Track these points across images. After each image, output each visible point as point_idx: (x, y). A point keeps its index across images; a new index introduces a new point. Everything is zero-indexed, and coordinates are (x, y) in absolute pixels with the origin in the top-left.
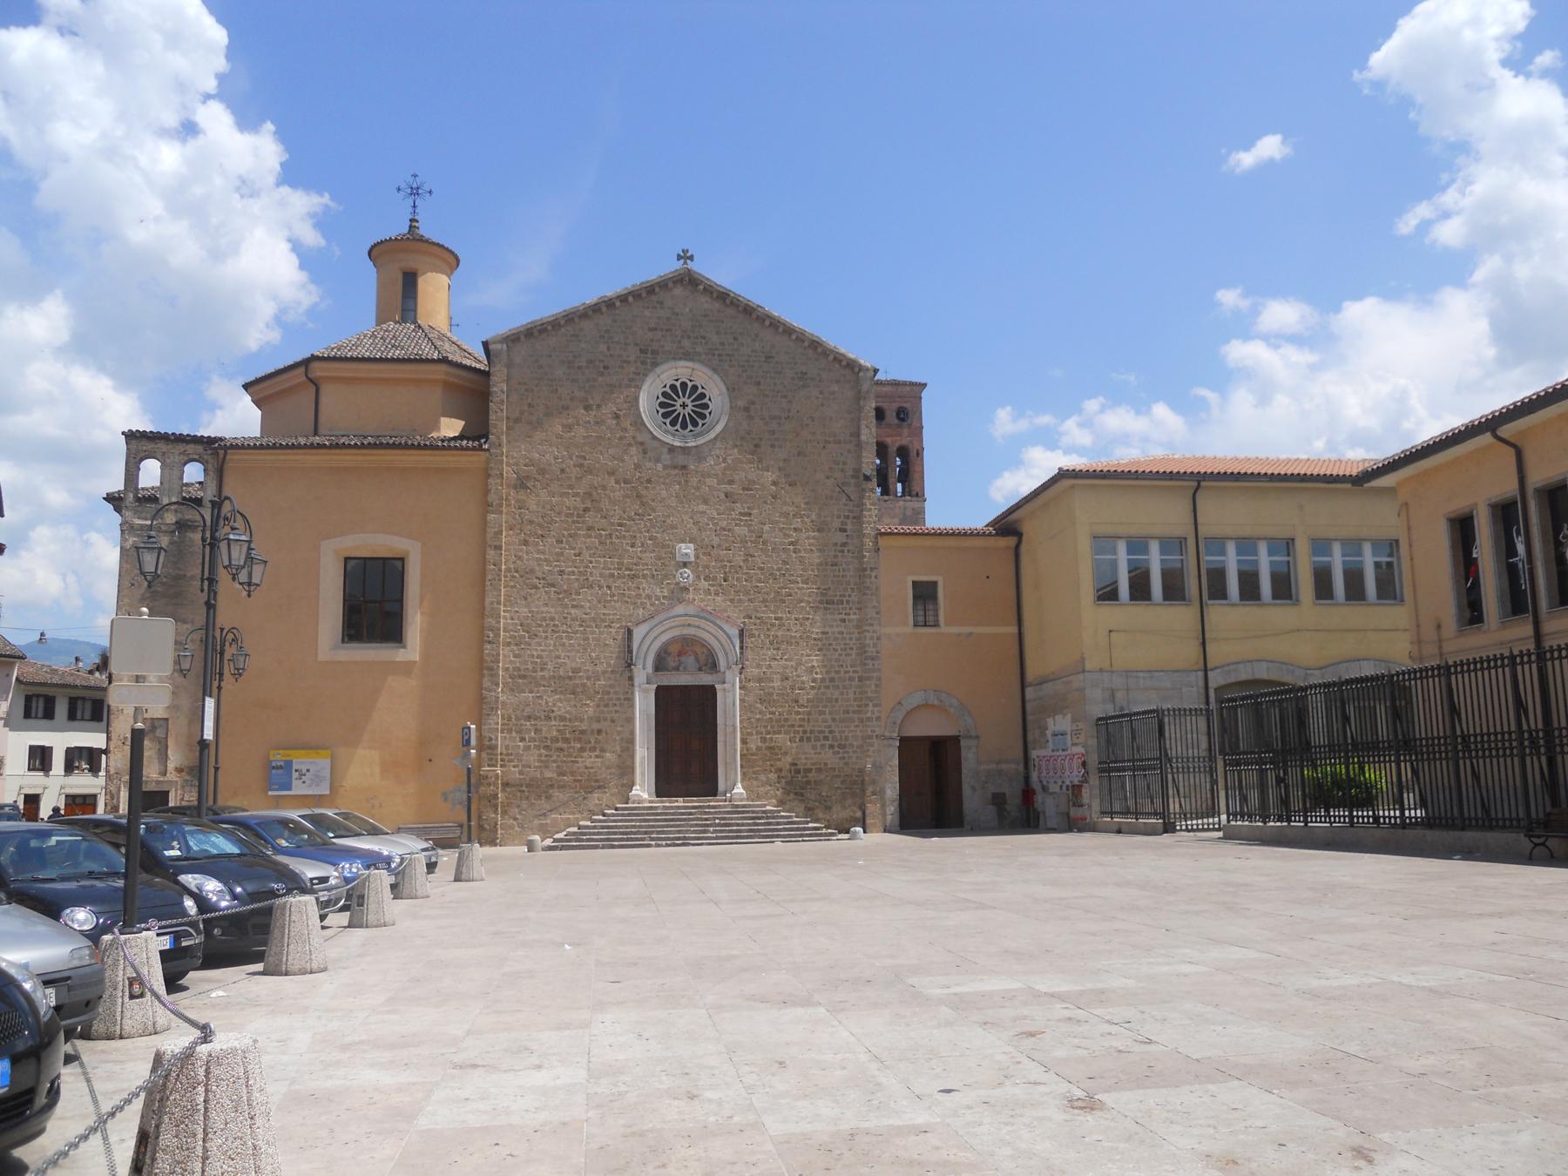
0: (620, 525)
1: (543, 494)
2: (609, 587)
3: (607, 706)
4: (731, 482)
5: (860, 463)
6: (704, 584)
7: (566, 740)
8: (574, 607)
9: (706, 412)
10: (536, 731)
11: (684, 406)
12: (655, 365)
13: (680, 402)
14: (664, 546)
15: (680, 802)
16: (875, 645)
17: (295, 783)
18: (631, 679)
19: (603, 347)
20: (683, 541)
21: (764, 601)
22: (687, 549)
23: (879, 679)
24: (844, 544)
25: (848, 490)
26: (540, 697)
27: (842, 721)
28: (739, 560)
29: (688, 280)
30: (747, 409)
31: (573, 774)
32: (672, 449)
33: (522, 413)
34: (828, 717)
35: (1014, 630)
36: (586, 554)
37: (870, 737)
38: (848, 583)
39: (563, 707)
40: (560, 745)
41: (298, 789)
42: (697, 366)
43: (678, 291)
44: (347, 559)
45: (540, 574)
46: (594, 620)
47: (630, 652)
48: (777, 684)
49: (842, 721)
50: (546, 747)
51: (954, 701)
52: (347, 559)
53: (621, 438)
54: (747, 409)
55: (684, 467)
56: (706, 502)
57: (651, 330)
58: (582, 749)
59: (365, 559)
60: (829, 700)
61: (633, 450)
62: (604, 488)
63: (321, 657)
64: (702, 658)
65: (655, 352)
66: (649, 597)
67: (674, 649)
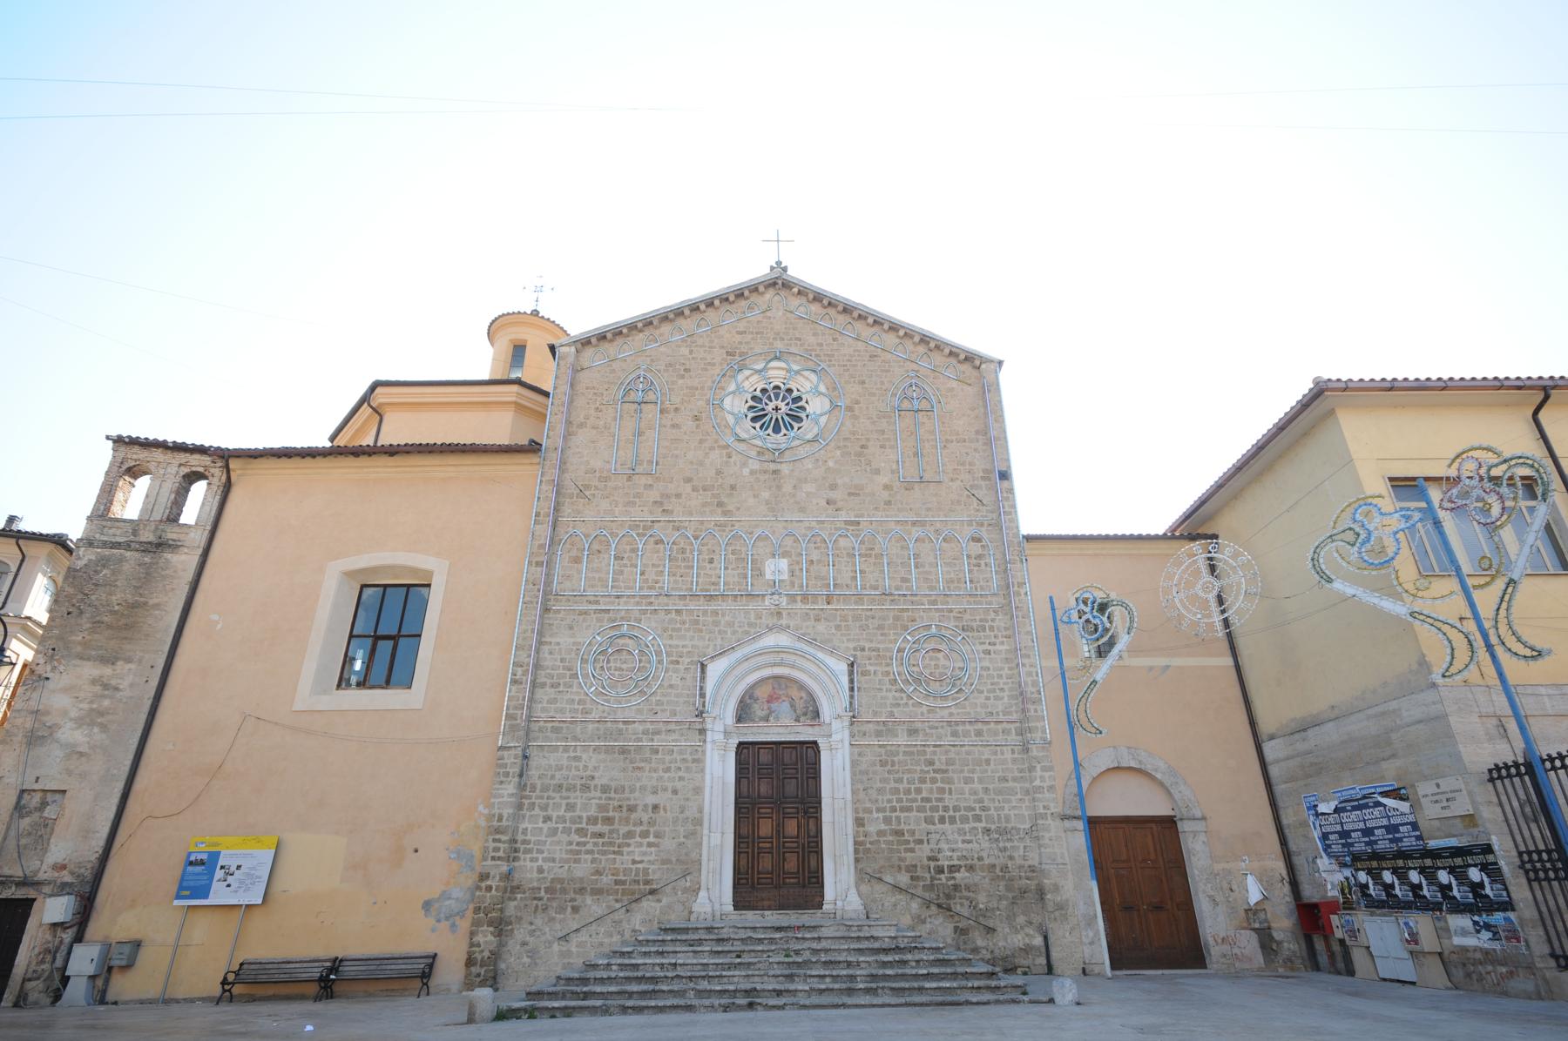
1: (605, 505)
3: (668, 770)
4: (833, 487)
7: (608, 820)
10: (570, 807)
17: (217, 887)
19: (685, 351)
21: (880, 627)
22: (776, 568)
24: (979, 557)
25: (980, 494)
27: (999, 792)
29: (779, 282)
30: (849, 409)
34: (977, 786)
35: (1230, 661)
37: (1044, 816)
39: (607, 772)
40: (599, 828)
41: (219, 894)
44: (363, 587)
47: (703, 695)
49: (999, 792)
50: (580, 832)
51: (1162, 765)
53: (701, 441)
54: (849, 409)
56: (802, 510)
57: (739, 333)
58: (630, 835)
59: (385, 586)
60: (978, 763)
64: (800, 705)
66: (730, 624)
67: (763, 693)
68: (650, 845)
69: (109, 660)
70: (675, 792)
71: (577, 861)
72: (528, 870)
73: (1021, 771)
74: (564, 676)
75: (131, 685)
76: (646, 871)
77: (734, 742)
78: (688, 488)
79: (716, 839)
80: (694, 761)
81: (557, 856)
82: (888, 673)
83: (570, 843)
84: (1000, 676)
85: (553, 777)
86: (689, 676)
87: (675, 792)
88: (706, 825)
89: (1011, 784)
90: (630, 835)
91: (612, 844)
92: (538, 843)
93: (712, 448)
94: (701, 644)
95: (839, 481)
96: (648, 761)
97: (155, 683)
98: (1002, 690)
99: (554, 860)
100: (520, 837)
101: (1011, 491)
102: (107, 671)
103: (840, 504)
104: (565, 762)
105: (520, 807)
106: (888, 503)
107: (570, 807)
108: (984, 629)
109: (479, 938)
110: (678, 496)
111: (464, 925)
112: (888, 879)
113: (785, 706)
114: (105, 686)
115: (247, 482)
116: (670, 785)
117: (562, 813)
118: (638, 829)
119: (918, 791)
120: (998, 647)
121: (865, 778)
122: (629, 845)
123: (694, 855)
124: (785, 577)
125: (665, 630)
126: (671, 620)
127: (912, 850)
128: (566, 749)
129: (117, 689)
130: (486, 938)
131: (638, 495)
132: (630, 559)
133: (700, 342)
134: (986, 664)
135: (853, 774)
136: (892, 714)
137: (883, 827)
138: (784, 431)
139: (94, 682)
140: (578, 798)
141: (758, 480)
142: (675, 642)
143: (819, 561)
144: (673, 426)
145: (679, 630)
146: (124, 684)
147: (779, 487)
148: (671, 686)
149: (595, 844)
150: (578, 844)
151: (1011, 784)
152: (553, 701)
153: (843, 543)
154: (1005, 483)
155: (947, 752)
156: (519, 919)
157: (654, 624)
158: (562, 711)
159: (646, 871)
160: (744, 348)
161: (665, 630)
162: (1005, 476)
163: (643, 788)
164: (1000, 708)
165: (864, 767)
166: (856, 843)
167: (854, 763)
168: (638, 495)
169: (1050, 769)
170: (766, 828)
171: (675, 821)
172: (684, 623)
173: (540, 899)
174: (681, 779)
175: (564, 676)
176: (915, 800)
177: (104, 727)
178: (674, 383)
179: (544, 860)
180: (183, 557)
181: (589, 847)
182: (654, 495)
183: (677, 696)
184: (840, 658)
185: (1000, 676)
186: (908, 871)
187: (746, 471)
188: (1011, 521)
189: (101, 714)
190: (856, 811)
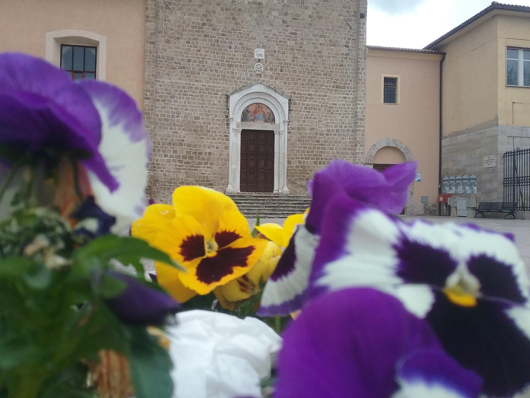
0: (223, 35)
1: (179, 13)
2: (216, 71)
3: (214, 139)
4: (286, 14)
5: (359, 8)
6: (269, 73)
7: (191, 158)
8: (196, 81)
10: (175, 152)
14: (247, 49)
15: (254, 194)
16: (362, 112)
18: (228, 124)
20: (258, 47)
21: (303, 84)
23: (364, 131)
24: (347, 54)
25: (351, 24)
26: (176, 133)
28: (289, 60)
36: (203, 52)
38: (348, 76)
40: (187, 160)
45: (177, 61)
46: (207, 89)
48: (308, 131)
50: (180, 161)
56: (272, 25)
58: (200, 163)
60: (336, 142)
62: (214, 12)
66: (239, 78)
67: (252, 109)
68: (208, 167)
70: (217, 148)
71: (180, 172)
72: (160, 174)
73: (352, 146)
74: (167, 97)
76: (207, 177)
78: (218, 9)
80: (225, 136)
82: (304, 104)
84: (349, 108)
85: (167, 139)
87: (217, 148)
89: (347, 151)
94: (226, 86)
95: (289, 12)
98: (349, 114)
99: (170, 172)
101: (364, 24)
103: (288, 23)
106: (310, 25)
107: (175, 152)
108: (345, 88)
112: (298, 183)
113: (261, 116)
116: (215, 145)
117: (172, 154)
118: (203, 162)
119: (312, 152)
120: (350, 96)
121: (292, 146)
122: (200, 167)
123: (226, 172)
124: (263, 58)
126: (213, 75)
127: (308, 174)
128: (171, 129)
131: (195, 10)
132: (193, 43)
134: (344, 103)
135: (288, 144)
136: (304, 122)
137: (298, 164)
140: (178, 148)
141: (251, 7)
143: (278, 51)
145: (217, 79)
147: (261, 12)
148: (214, 104)
150: (179, 166)
151: (347, 151)
153: (289, 43)
154: (363, 19)
155: (325, 137)
157: (206, 76)
158: (168, 112)
162: (363, 16)
163: (204, 146)
164: (347, 122)
165: (291, 142)
167: (289, 140)
168: (195, 10)
169: (363, 146)
170: (252, 164)
173: (166, 185)
175: (167, 97)
176: (311, 155)
179: (166, 171)
181: (184, 167)
182: (202, 11)
183: (217, 108)
184: (286, 97)
185: (349, 108)
188: (363, 39)
190: (288, 158)
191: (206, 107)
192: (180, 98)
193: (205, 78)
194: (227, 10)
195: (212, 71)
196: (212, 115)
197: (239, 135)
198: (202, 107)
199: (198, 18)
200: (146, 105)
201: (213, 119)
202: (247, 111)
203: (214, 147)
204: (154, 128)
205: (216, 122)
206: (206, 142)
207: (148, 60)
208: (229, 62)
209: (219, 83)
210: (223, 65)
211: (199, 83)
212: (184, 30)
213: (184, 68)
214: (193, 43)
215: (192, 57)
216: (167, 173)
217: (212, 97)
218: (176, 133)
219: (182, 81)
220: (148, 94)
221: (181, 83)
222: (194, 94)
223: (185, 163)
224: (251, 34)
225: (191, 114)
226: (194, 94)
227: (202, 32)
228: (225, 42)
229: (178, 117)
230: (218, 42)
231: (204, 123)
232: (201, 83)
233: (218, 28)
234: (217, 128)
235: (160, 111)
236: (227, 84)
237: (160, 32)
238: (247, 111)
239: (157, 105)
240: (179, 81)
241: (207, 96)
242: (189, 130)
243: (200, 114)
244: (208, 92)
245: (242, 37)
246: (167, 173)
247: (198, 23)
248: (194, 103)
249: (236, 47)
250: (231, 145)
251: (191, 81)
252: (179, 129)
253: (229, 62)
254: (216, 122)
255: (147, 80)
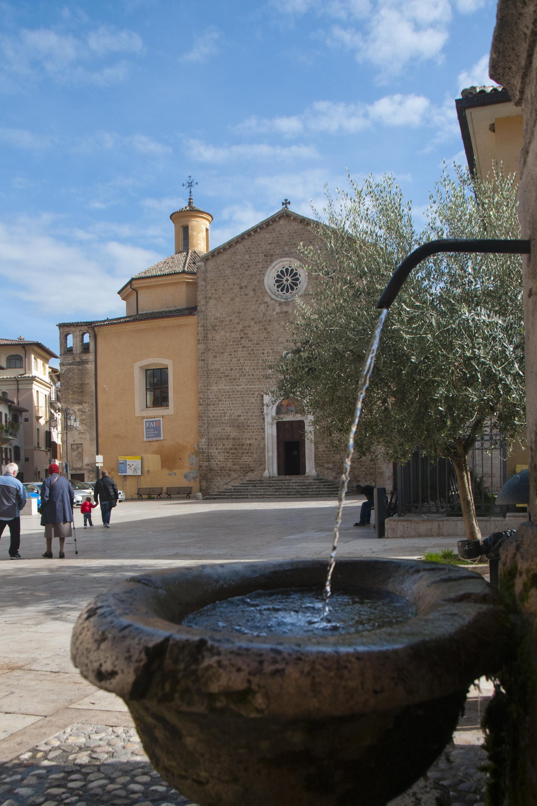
0: (257, 344)
1: (223, 333)
2: (253, 375)
3: (253, 432)
7: (236, 449)
9: (298, 282)
10: (224, 445)
11: (287, 280)
12: (272, 262)
13: (285, 278)
17: (128, 470)
18: (264, 419)
19: (247, 257)
26: (224, 429)
29: (285, 215)
31: (240, 465)
32: (280, 304)
33: (212, 294)
36: (242, 361)
40: (233, 451)
42: (292, 259)
43: (282, 222)
44: (147, 370)
45: (222, 371)
46: (246, 391)
50: (227, 452)
52: (147, 370)
53: (256, 301)
55: (286, 312)
57: (269, 244)
58: (243, 453)
59: (153, 369)
61: (262, 307)
63: (137, 415)
65: (272, 255)
68: (249, 456)
69: (80, 403)
70: (256, 439)
71: (228, 462)
74: (216, 401)
75: (89, 411)
77: (276, 421)
79: (270, 454)
81: (222, 460)
83: (225, 456)
85: (217, 436)
86: (258, 399)
87: (256, 439)
88: (266, 450)
90: (243, 453)
91: (237, 456)
92: (215, 456)
93: (261, 304)
94: (261, 387)
96: (247, 429)
97: (94, 410)
100: (210, 455)
102: (81, 407)
104: (220, 430)
105: (208, 445)
109: (202, 484)
110: (249, 326)
111: (198, 480)
114: (82, 412)
115: (101, 332)
117: (221, 447)
118: (245, 451)
125: (249, 382)
128: (220, 427)
129: (85, 412)
130: (204, 483)
131: (235, 328)
132: (234, 355)
133: (253, 252)
138: (290, 291)
139: (79, 410)
140: (226, 442)
141: (279, 317)
142: (252, 387)
144: (246, 295)
146: (87, 410)
148: (252, 403)
149: (233, 456)
152: (214, 410)
156: (213, 479)
157: (244, 380)
158: (217, 413)
159: (249, 464)
160: (272, 252)
161: (249, 382)
163: (246, 438)
166: (315, 455)
168: (235, 328)
171: (257, 449)
172: (255, 379)
174: (258, 435)
175: (216, 401)
177: (86, 425)
178: (244, 273)
179: (218, 461)
180: (90, 366)
181: (231, 457)
182: (240, 327)
183: (254, 406)
186: (332, 463)
187: (275, 313)
189: (84, 420)
191: (247, 406)
192: (226, 401)
193: (244, 382)
194: (259, 323)
195: (249, 375)
196: (250, 412)
197: (275, 427)
198: (243, 406)
199: (238, 333)
200: (200, 410)
201: (252, 416)
202: (281, 405)
203: (253, 438)
204: (208, 427)
205: (254, 417)
206: (247, 435)
207: (200, 374)
208: (262, 366)
209: (255, 385)
210: (258, 369)
211: (239, 387)
212: (227, 345)
213: (228, 376)
214: (234, 355)
215: (234, 366)
216: (219, 463)
217: (250, 397)
218: (224, 429)
219: (227, 387)
220: (201, 401)
221: (226, 389)
222: (236, 396)
223: (232, 453)
224: (280, 340)
225: (234, 413)
226: (236, 396)
227: (241, 344)
228: (259, 350)
229: (225, 416)
230: (253, 351)
231: (245, 419)
232: (241, 387)
233: (253, 339)
234: (255, 423)
235: (211, 413)
236: (262, 384)
237: (209, 350)
238: (281, 405)
239: (209, 409)
240: (225, 387)
241: (246, 397)
242: (233, 427)
243: (242, 412)
244: (246, 393)
245: (272, 343)
246: (219, 463)
247: (237, 338)
248: (237, 404)
249: (268, 352)
250: (266, 436)
251: (234, 386)
252: (226, 426)
253: (262, 366)
254: (254, 417)
255: (200, 390)
